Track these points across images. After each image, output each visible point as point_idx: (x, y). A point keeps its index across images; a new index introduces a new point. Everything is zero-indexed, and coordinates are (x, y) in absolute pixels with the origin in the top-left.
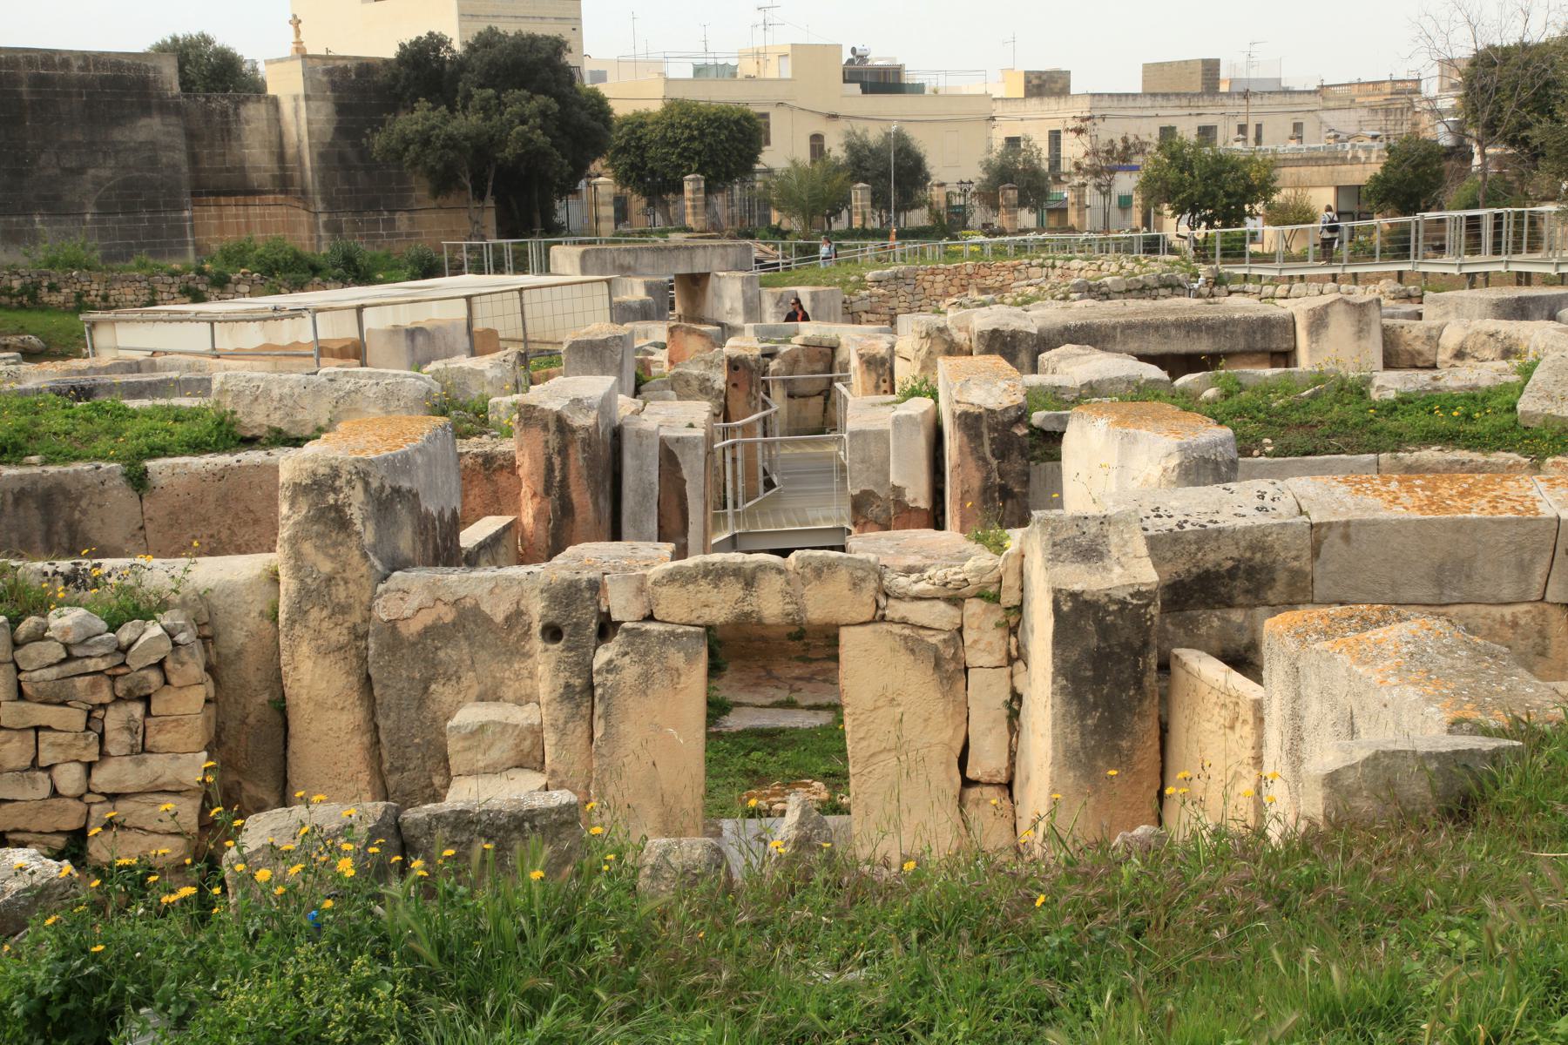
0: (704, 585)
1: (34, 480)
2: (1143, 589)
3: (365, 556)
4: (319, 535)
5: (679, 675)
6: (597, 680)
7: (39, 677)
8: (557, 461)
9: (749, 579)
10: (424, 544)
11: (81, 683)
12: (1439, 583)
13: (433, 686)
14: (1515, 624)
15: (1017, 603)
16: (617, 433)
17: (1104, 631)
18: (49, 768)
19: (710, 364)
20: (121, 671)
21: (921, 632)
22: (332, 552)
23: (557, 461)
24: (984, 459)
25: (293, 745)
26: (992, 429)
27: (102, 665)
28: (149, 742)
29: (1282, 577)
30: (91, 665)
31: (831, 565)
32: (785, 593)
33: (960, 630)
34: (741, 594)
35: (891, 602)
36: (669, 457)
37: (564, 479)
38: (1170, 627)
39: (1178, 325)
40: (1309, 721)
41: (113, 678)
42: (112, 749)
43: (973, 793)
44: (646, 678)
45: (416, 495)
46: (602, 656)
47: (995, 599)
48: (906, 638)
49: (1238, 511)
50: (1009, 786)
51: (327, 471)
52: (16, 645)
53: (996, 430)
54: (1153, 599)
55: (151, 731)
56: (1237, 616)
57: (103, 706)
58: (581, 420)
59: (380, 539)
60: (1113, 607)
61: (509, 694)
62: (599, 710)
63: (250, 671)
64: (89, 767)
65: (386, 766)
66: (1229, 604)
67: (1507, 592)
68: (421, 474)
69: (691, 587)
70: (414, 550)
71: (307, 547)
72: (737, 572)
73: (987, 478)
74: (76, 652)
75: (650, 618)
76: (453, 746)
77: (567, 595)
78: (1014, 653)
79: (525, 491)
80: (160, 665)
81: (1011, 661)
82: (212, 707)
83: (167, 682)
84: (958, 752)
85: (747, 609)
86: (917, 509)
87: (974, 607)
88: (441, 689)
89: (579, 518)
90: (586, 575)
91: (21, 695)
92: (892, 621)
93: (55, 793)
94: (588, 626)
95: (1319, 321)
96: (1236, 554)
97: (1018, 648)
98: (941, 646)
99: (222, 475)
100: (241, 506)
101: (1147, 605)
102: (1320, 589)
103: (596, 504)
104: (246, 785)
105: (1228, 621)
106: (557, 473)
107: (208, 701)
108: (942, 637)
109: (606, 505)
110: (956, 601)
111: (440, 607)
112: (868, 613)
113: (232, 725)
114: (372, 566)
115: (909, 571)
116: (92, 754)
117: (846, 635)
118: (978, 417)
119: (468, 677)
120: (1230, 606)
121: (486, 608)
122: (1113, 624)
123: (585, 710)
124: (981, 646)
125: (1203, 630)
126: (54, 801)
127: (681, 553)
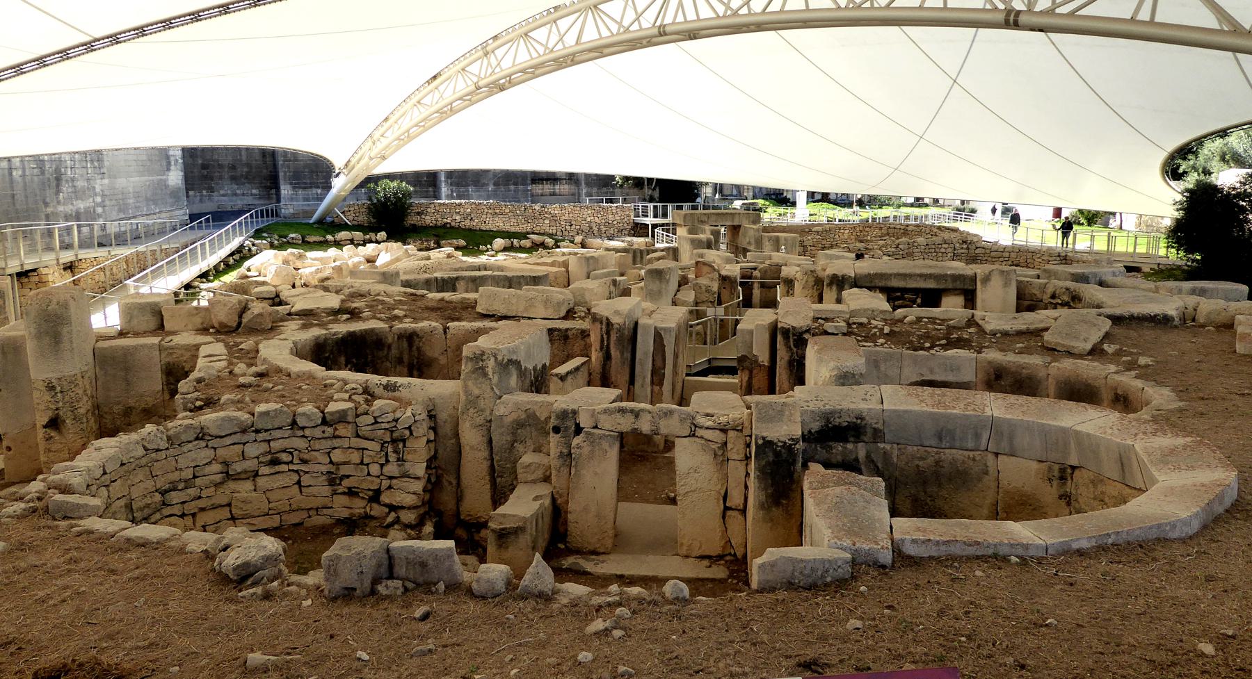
0: (618, 415)
1: (405, 330)
7: (365, 431)
9: (637, 414)
12: (940, 439)
14: (974, 460)
16: (636, 323)
17: (777, 454)
19: (712, 279)
27: (387, 426)
29: (870, 431)
31: (671, 412)
36: (658, 336)
39: (921, 276)
41: (392, 432)
43: (729, 513)
44: (592, 452)
46: (576, 441)
47: (741, 431)
52: (357, 416)
56: (850, 446)
58: (616, 320)
59: (500, 381)
63: (446, 430)
64: (382, 465)
66: (847, 441)
67: (970, 445)
71: (470, 383)
72: (632, 411)
75: (596, 427)
76: (519, 470)
77: (564, 415)
80: (409, 428)
82: (432, 445)
87: (731, 434)
90: (572, 407)
91: (358, 436)
93: (369, 474)
95: (987, 279)
102: (887, 437)
109: (628, 355)
110: (724, 431)
113: (440, 451)
115: (707, 415)
118: (788, 330)
119: (529, 442)
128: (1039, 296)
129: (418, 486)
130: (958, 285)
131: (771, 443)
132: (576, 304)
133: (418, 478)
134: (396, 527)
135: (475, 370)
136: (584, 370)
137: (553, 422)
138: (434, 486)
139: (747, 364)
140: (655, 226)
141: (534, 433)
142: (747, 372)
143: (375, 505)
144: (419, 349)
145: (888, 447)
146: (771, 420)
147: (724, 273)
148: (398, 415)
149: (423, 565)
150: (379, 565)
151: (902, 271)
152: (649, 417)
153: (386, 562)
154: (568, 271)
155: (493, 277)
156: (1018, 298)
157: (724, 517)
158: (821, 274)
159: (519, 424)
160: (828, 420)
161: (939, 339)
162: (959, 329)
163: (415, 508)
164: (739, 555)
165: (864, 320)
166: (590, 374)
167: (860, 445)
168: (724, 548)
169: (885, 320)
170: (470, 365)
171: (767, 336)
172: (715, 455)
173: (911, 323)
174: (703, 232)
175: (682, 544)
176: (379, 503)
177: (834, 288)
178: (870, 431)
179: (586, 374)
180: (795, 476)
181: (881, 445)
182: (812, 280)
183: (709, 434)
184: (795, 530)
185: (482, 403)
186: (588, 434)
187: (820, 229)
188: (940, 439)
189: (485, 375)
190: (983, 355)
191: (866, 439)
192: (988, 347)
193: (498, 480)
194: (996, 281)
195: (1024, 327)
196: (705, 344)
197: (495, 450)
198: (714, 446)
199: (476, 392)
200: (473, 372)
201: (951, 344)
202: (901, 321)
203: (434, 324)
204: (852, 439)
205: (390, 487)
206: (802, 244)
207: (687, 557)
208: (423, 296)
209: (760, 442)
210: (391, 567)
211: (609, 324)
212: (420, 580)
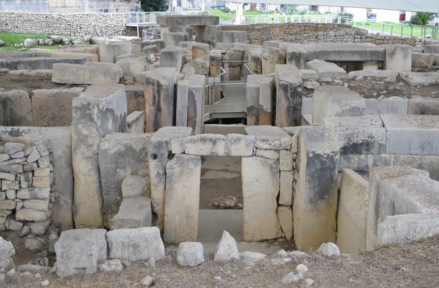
0: (201, 143)
2: (334, 151)
3: (98, 130)
4: (85, 123)
5: (192, 170)
6: (167, 171)
8: (157, 95)
10: (116, 125)
11: (14, 166)
12: (423, 149)
13: (118, 170)
15: (296, 152)
16: (175, 86)
18: (5, 191)
19: (206, 59)
20: (25, 163)
21: (267, 160)
22: (88, 128)
23: (157, 95)
24: (288, 98)
25: (76, 186)
26: (291, 89)
27: (20, 161)
28: (34, 185)
29: (376, 146)
30: (17, 161)
32: (225, 147)
33: (279, 159)
34: (212, 146)
35: (258, 150)
37: (159, 100)
38: (342, 160)
39: (350, 52)
40: (382, 201)
42: (22, 185)
43: (281, 208)
44: (182, 171)
45: (113, 111)
46: (169, 164)
48: (262, 161)
49: (365, 125)
50: (292, 206)
51: (86, 103)
53: (292, 89)
54: (337, 154)
55: (34, 181)
56: (363, 157)
57: (20, 173)
58: (163, 82)
59: (102, 124)
60: (325, 156)
61: (140, 173)
62: (168, 180)
65: (103, 193)
66: (361, 153)
68: (115, 104)
69: (196, 144)
70: (112, 127)
71: (80, 126)
72: (211, 140)
73: (289, 104)
74: (13, 157)
75: (184, 153)
77: (159, 145)
78: (295, 167)
79: (147, 105)
80: (37, 161)
81: (294, 169)
83: (38, 166)
84: (276, 196)
85: (214, 151)
86: (267, 112)
87: (283, 152)
88: (120, 171)
89: (163, 113)
90: (164, 139)
92: (258, 156)
93: (6, 198)
94: (165, 155)
95: (393, 54)
96: (363, 139)
97: (296, 166)
98: (272, 164)
99: (55, 95)
100: (61, 105)
101: (335, 156)
103: (168, 108)
104: (61, 196)
105: (360, 158)
106: (157, 99)
107: (51, 172)
108: (273, 161)
109: (171, 108)
110: (278, 151)
111: (120, 146)
112: (251, 153)
113: (57, 179)
114: (100, 133)
116: (17, 188)
117: (243, 159)
118: (287, 86)
120: (360, 154)
121: (133, 147)
122: (325, 161)
123: (163, 180)
124: (285, 164)
125: (352, 161)
126: (7, 201)
127: (193, 133)
128: (425, 64)
129: (44, 205)
130: (374, 58)
131: (318, 155)
132: (125, 74)
133: (44, 199)
134: (30, 236)
135: (83, 117)
136: (142, 118)
137: (151, 150)
138: (54, 203)
139: (255, 111)
140: (141, 28)
141: (132, 161)
142: (254, 118)
143: (12, 222)
144: (11, 110)
145: (387, 156)
146: (316, 139)
147: (212, 55)
148: (28, 152)
149: (136, 247)
150: (101, 250)
151: (337, 49)
152: (223, 143)
153: (106, 247)
154: (99, 56)
155: (45, 61)
156: (412, 66)
157: (277, 212)
158: (283, 53)
159: (120, 154)
160: (349, 140)
161: (382, 90)
162: (393, 83)
163: (43, 221)
164: (288, 237)
165: (330, 80)
166: (145, 123)
167: (370, 156)
168: (277, 233)
169: (342, 79)
170: (79, 113)
171: (269, 92)
172: (271, 168)
173: (360, 81)
174: (181, 30)
175: (247, 233)
176: (14, 218)
177: (294, 62)
178: (376, 146)
179: (143, 123)
180: (334, 178)
181: (383, 155)
182: (276, 57)
183: (267, 154)
184: (333, 216)
185: (90, 141)
186: (179, 158)
187: (260, 27)
188: (423, 149)
189: (92, 120)
190: (412, 99)
191: (374, 152)
192: (414, 94)
193: (105, 197)
194: (399, 55)
195: (434, 81)
196: (208, 104)
197: (102, 175)
198: (271, 162)
199: (85, 132)
200: (83, 118)
201: (389, 94)
202: (354, 79)
203: (22, 91)
204: (364, 152)
205: (23, 207)
206: (248, 37)
207: (250, 241)
208: (6, 72)
209: (311, 155)
210: (109, 250)
211: (159, 85)
212: (134, 259)
